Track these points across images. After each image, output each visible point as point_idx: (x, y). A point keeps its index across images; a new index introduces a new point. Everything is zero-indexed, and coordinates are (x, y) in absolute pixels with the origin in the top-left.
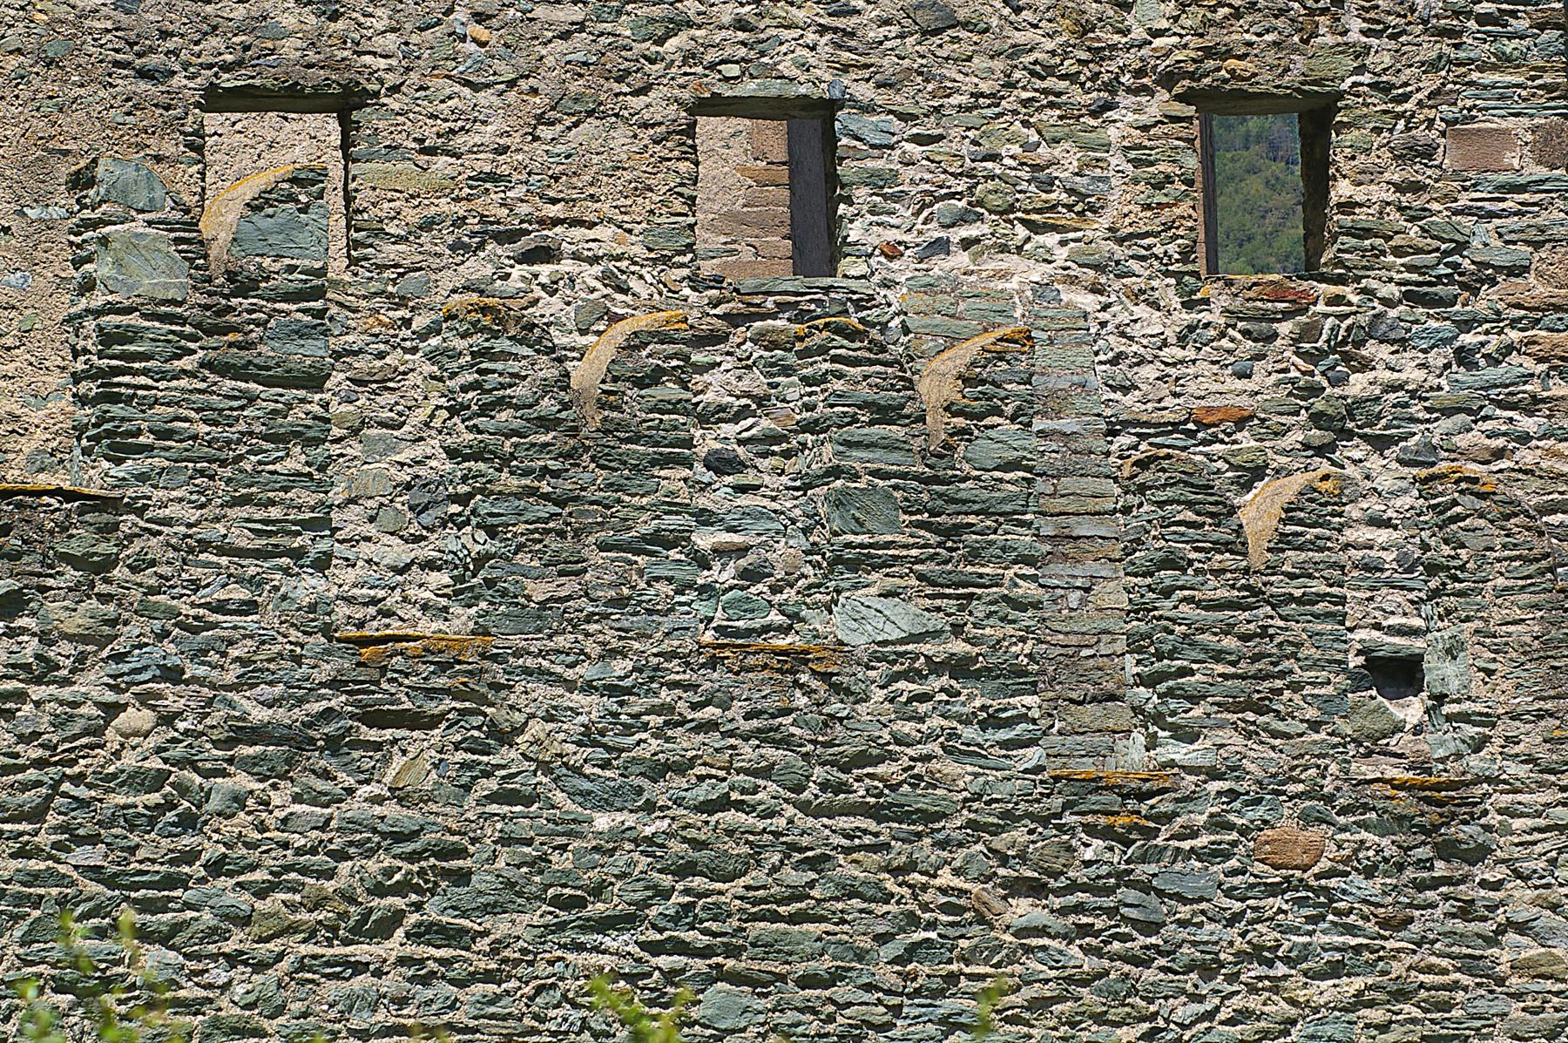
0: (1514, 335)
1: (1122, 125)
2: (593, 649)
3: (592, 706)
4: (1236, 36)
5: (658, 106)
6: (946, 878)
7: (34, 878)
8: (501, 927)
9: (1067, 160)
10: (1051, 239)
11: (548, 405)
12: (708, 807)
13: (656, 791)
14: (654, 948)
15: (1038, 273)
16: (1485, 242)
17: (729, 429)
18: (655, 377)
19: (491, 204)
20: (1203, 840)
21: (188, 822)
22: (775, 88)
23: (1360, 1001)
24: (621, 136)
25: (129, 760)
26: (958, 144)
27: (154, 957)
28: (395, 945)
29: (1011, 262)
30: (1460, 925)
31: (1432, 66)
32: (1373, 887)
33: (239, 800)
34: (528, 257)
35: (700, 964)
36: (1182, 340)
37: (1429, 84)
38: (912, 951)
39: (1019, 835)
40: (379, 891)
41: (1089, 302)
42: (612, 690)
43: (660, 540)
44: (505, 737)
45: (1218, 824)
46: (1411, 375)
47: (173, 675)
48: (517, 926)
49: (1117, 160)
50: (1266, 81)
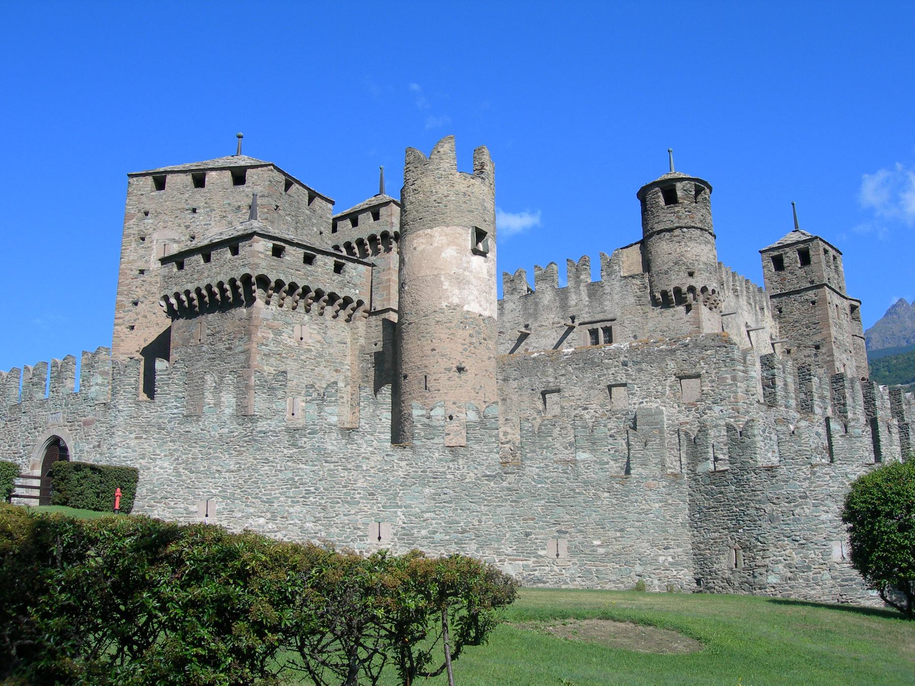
0: (729, 407)
1: (668, 382)
2: (538, 462)
4: (685, 366)
5: (601, 387)
6: (593, 491)
7: (456, 496)
8: (524, 500)
9: (660, 388)
10: (658, 400)
11: (530, 429)
12: (555, 483)
14: (546, 502)
15: (656, 405)
17: (613, 431)
19: (579, 403)
20: (636, 484)
22: (618, 382)
24: (596, 392)
25: (470, 480)
29: (651, 404)
30: (680, 495)
31: (714, 369)
33: (486, 484)
34: (583, 410)
35: (555, 504)
36: (678, 413)
37: (714, 371)
39: (606, 485)
40: (506, 496)
41: (664, 408)
42: (541, 468)
43: (547, 448)
47: (476, 468)
49: (668, 388)
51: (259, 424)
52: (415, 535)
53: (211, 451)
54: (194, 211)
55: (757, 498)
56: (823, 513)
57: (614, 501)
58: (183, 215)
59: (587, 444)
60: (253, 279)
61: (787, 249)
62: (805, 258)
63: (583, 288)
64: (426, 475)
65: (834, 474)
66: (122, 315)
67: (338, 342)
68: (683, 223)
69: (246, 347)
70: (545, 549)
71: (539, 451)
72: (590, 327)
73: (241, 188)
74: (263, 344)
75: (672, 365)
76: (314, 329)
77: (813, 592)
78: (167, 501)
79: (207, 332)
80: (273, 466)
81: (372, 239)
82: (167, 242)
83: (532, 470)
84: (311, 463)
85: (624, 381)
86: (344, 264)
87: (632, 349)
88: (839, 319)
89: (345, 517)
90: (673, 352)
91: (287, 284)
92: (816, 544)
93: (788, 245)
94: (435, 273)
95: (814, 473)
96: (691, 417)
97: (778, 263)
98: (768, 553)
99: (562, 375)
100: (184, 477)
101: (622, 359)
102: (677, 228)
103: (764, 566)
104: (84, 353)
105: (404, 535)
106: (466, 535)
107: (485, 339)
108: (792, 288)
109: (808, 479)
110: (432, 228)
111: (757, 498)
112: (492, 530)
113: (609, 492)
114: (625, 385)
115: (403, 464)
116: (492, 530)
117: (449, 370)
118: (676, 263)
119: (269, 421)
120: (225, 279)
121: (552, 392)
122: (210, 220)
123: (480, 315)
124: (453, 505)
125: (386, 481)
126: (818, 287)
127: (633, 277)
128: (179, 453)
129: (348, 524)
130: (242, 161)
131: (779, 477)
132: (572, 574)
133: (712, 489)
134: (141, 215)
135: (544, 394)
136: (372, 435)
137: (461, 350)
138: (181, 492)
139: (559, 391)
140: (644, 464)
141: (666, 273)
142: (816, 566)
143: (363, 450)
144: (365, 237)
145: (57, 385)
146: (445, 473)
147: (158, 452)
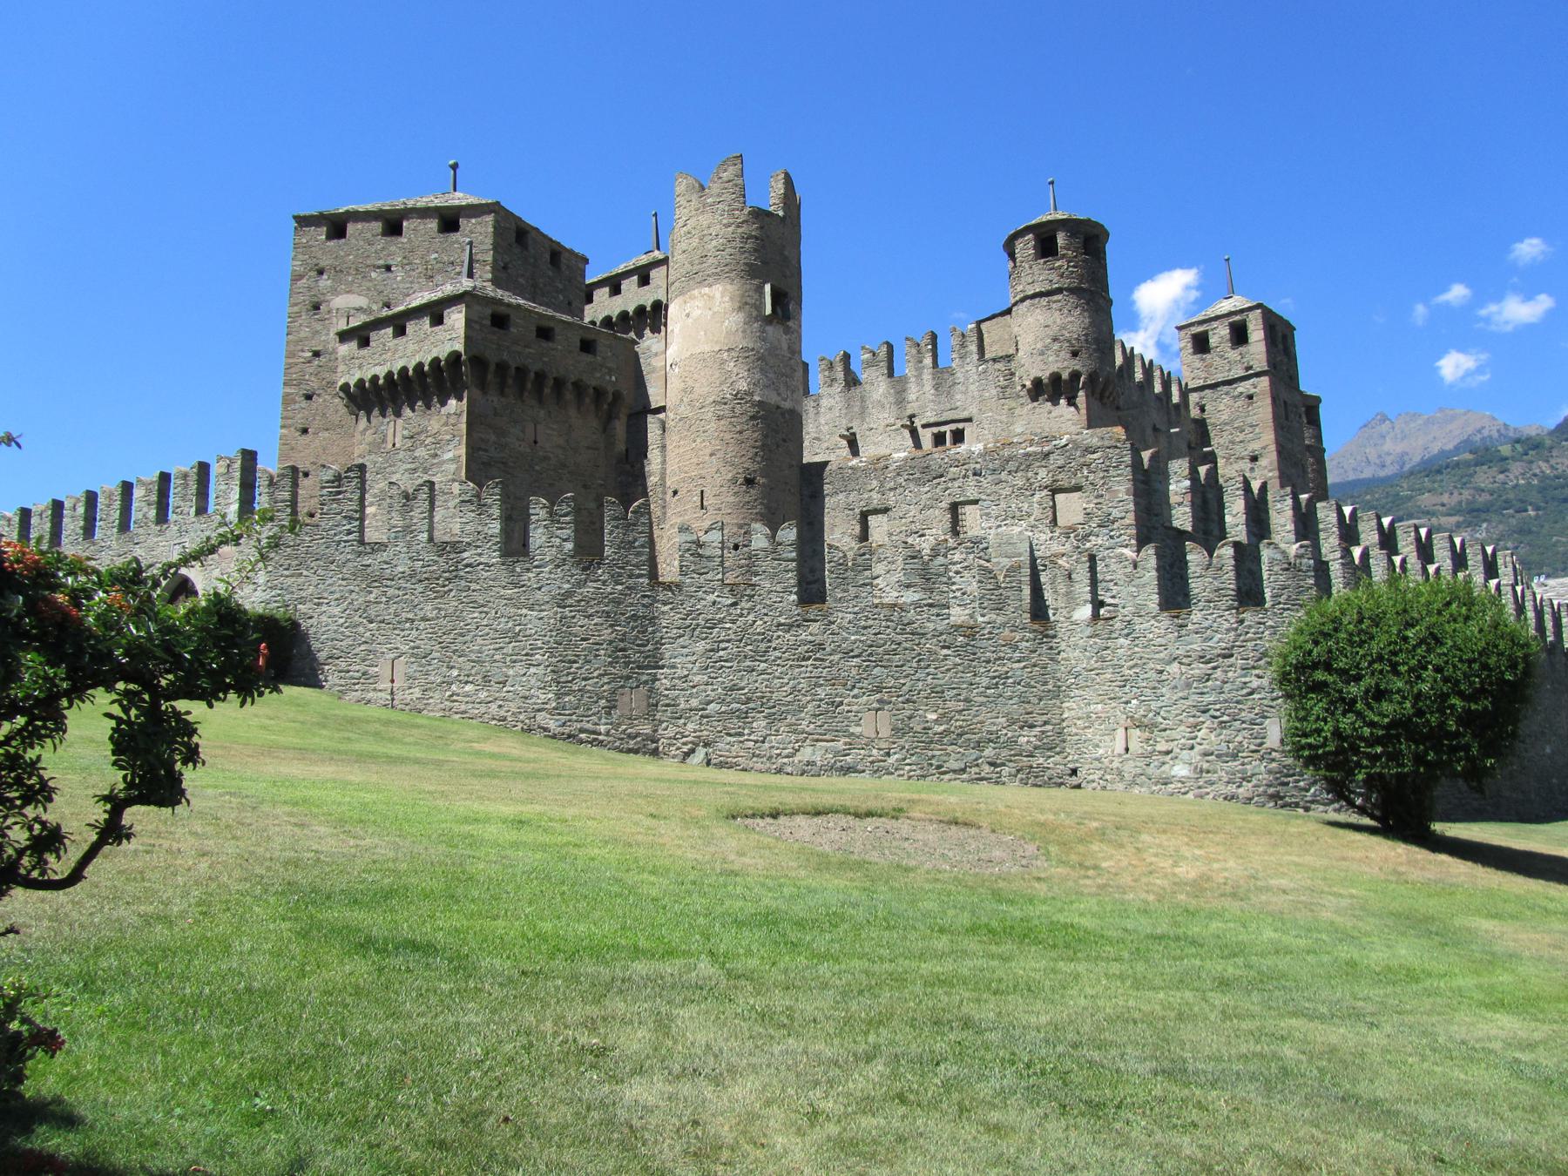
3: (851, 616)
4: (1060, 477)
5: (944, 505)
13: (865, 632)
15: (1019, 529)
16: (1116, 513)
18: (864, 554)
19: (913, 527)
21: (769, 641)
23: (1025, 667)
26: (1003, 505)
27: (763, 665)
28: (810, 662)
32: (1028, 644)
33: (779, 637)
38: (919, 661)
44: (833, 623)
45: (990, 633)
46: (1100, 542)
47: (766, 615)
48: (836, 657)
50: (1066, 485)
51: (465, 555)
52: (682, 706)
53: (397, 592)
54: (388, 268)
55: (1157, 656)
56: (1253, 678)
57: (957, 660)
58: (373, 275)
59: (917, 580)
60: (463, 357)
61: (1215, 324)
62: (1239, 335)
63: (927, 376)
64: (698, 625)
65: (1270, 623)
66: (290, 414)
67: (588, 448)
68: (1066, 283)
69: (457, 453)
70: (860, 725)
71: (853, 591)
72: (935, 430)
73: (454, 236)
74: (480, 449)
75: (1042, 473)
76: (553, 429)
77: (1241, 790)
78: (337, 661)
79: (406, 432)
80: (487, 613)
81: (641, 310)
82: (352, 312)
83: (843, 617)
84: (537, 607)
85: (976, 496)
86: (594, 341)
87: (985, 453)
88: (1287, 419)
89: (584, 683)
90: (1047, 455)
91: (513, 365)
92: (1243, 722)
93: (1217, 318)
94: (717, 349)
95: (1242, 622)
96: (1068, 545)
97: (1201, 344)
98: (1174, 734)
99: (891, 489)
100: (361, 629)
101: (973, 466)
102: (1059, 291)
103: (1168, 753)
104: (220, 458)
105: (668, 705)
106: (752, 705)
107: (784, 441)
108: (1220, 377)
109: (1236, 629)
110: (710, 286)
111: (1157, 656)
112: (788, 699)
113: (948, 648)
114: (976, 502)
115: (666, 608)
116: (788, 699)
117: (734, 481)
118: (1055, 340)
119: (479, 551)
120: (427, 359)
121: (876, 512)
122: (411, 282)
123: (778, 407)
124: (735, 664)
125: (643, 632)
126: (1258, 375)
127: (994, 360)
128: (354, 596)
129: (588, 691)
130: (460, 198)
131: (1190, 627)
132: (897, 760)
133: (1096, 643)
134: (313, 273)
135: (864, 517)
136: (623, 568)
137: (750, 455)
138: (357, 650)
139: (886, 510)
140: (999, 607)
141: (1042, 353)
142: (1244, 754)
143: (609, 589)
144: (631, 309)
145: (182, 504)
146: (721, 621)
147: (325, 595)
